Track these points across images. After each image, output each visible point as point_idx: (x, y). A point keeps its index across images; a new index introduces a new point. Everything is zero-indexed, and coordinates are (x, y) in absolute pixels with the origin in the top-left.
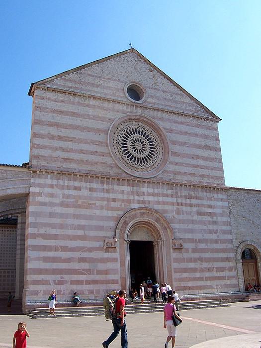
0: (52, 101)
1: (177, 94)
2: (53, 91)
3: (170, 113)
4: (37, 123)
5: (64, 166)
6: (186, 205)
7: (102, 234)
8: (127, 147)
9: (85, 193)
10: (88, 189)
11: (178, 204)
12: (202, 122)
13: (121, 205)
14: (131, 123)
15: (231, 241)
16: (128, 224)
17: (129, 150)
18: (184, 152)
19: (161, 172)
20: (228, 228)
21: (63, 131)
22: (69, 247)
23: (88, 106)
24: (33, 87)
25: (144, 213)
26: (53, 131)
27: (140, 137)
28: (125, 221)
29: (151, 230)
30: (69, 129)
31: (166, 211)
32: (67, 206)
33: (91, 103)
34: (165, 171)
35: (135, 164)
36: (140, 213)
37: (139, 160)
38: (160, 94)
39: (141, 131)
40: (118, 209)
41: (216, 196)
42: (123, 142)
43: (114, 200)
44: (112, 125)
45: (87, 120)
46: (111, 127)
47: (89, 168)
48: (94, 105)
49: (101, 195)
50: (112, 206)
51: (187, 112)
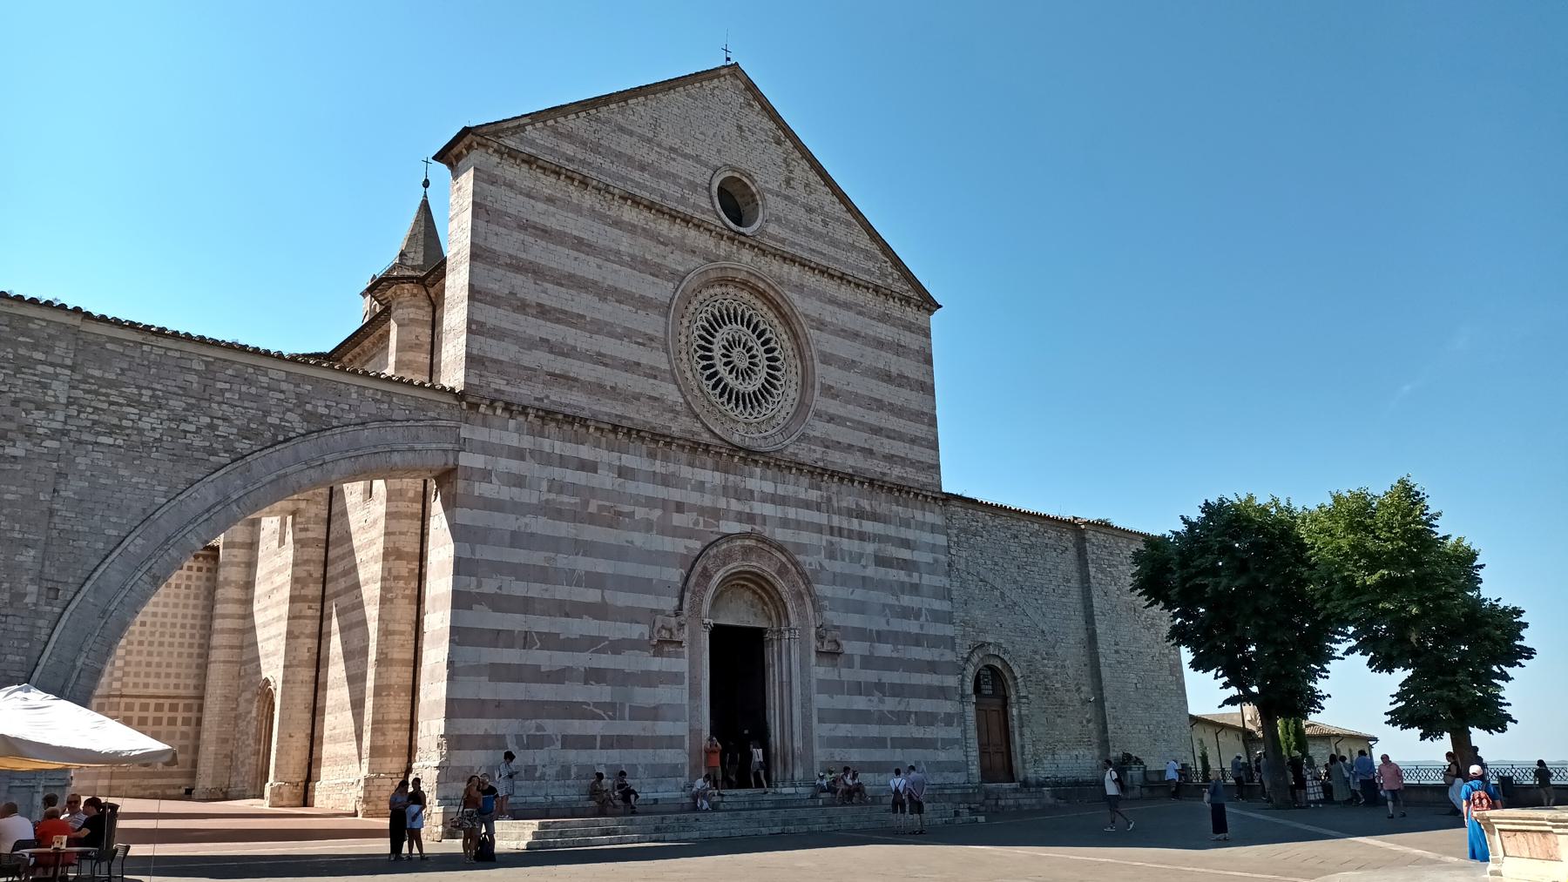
0: (521, 193)
1: (838, 219)
2: (524, 161)
3: (822, 272)
4: (478, 256)
5: (552, 398)
6: (851, 534)
7: (648, 602)
8: (710, 358)
9: (605, 479)
10: (616, 471)
11: (832, 530)
13: (696, 523)
14: (724, 290)
16: (710, 577)
17: (718, 368)
18: (849, 388)
19: (794, 438)
20: (944, 606)
21: (550, 292)
22: (562, 637)
23: (617, 223)
24: (466, 141)
25: (751, 549)
26: (527, 288)
27: (746, 333)
28: (705, 568)
29: (761, 597)
30: (569, 287)
31: (801, 548)
32: (557, 513)
33: (626, 218)
34: (804, 437)
36: (742, 547)
37: (740, 399)
38: (798, 215)
39: (747, 315)
40: (689, 534)
41: (918, 515)
42: (703, 343)
43: (680, 507)
44: (680, 290)
45: (616, 267)
46: (676, 297)
47: (619, 409)
48: (634, 226)
49: (648, 489)
50: (674, 524)
51: (861, 276)
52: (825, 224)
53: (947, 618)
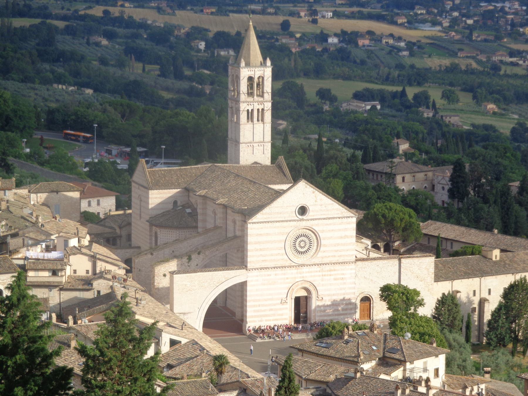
6: (327, 275)
11: (323, 275)
12: (345, 220)
15: (354, 293)
20: (353, 285)
35: (300, 256)
43: (287, 278)
52: (325, 207)
53: (354, 288)
